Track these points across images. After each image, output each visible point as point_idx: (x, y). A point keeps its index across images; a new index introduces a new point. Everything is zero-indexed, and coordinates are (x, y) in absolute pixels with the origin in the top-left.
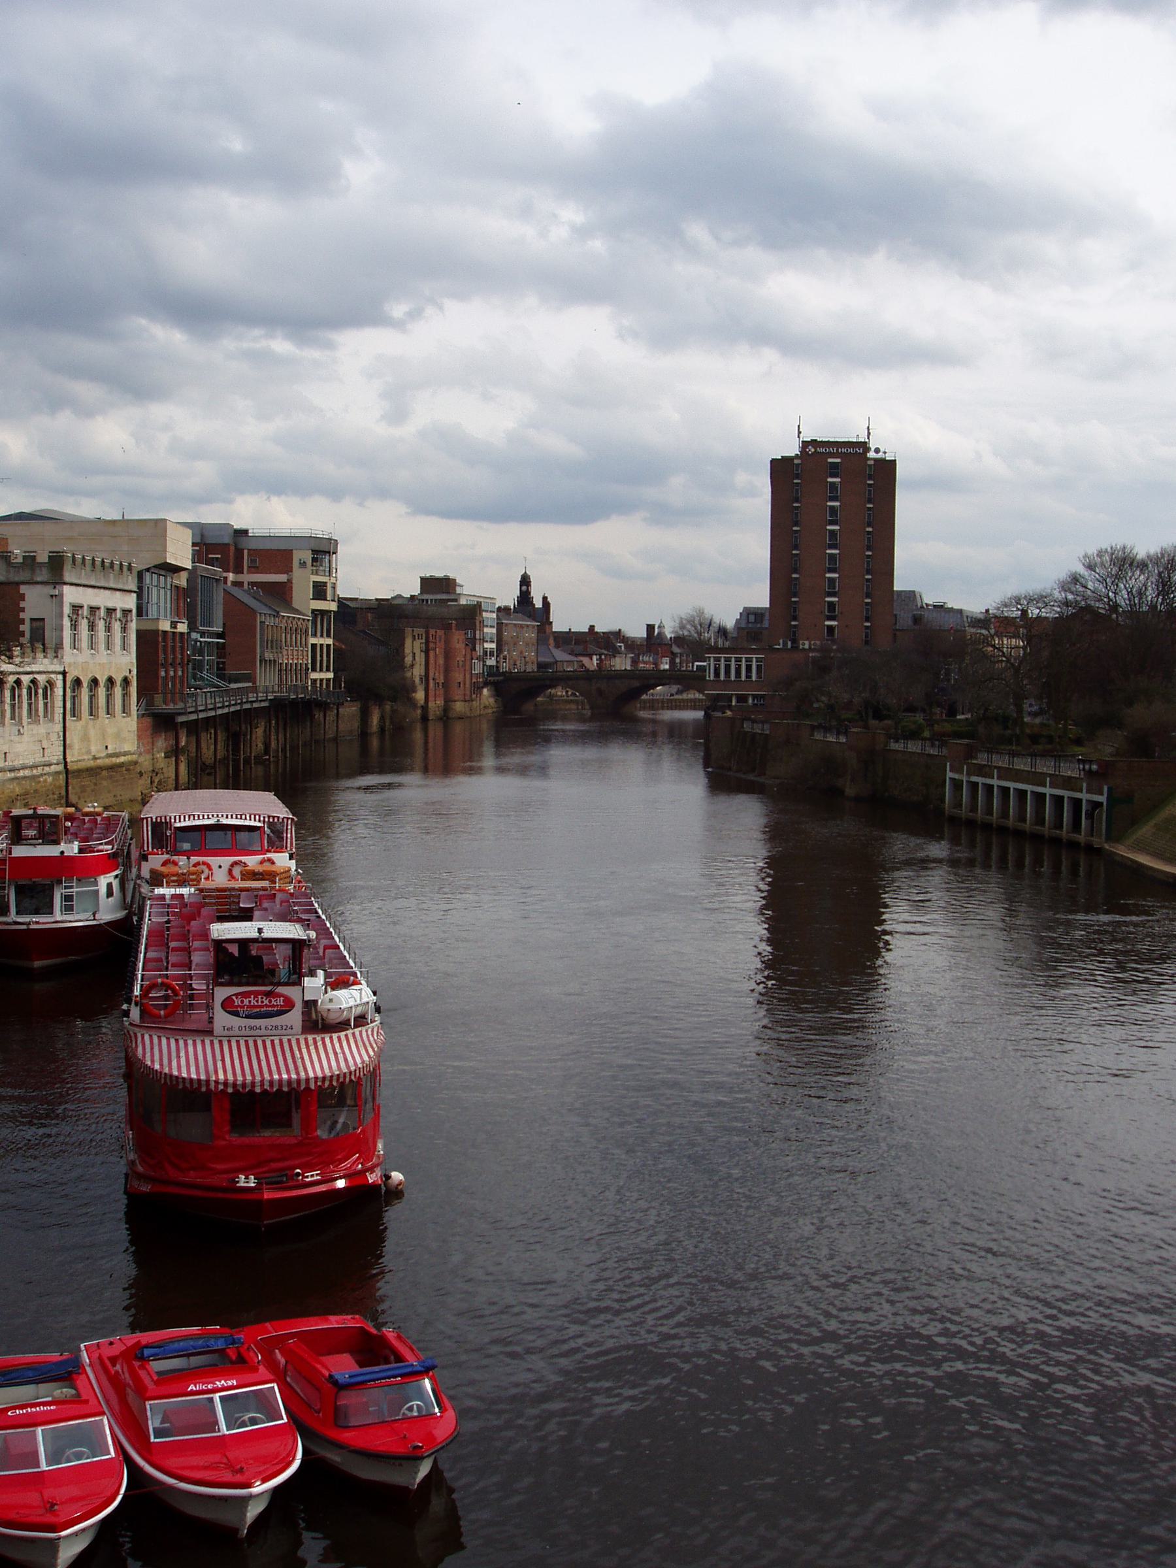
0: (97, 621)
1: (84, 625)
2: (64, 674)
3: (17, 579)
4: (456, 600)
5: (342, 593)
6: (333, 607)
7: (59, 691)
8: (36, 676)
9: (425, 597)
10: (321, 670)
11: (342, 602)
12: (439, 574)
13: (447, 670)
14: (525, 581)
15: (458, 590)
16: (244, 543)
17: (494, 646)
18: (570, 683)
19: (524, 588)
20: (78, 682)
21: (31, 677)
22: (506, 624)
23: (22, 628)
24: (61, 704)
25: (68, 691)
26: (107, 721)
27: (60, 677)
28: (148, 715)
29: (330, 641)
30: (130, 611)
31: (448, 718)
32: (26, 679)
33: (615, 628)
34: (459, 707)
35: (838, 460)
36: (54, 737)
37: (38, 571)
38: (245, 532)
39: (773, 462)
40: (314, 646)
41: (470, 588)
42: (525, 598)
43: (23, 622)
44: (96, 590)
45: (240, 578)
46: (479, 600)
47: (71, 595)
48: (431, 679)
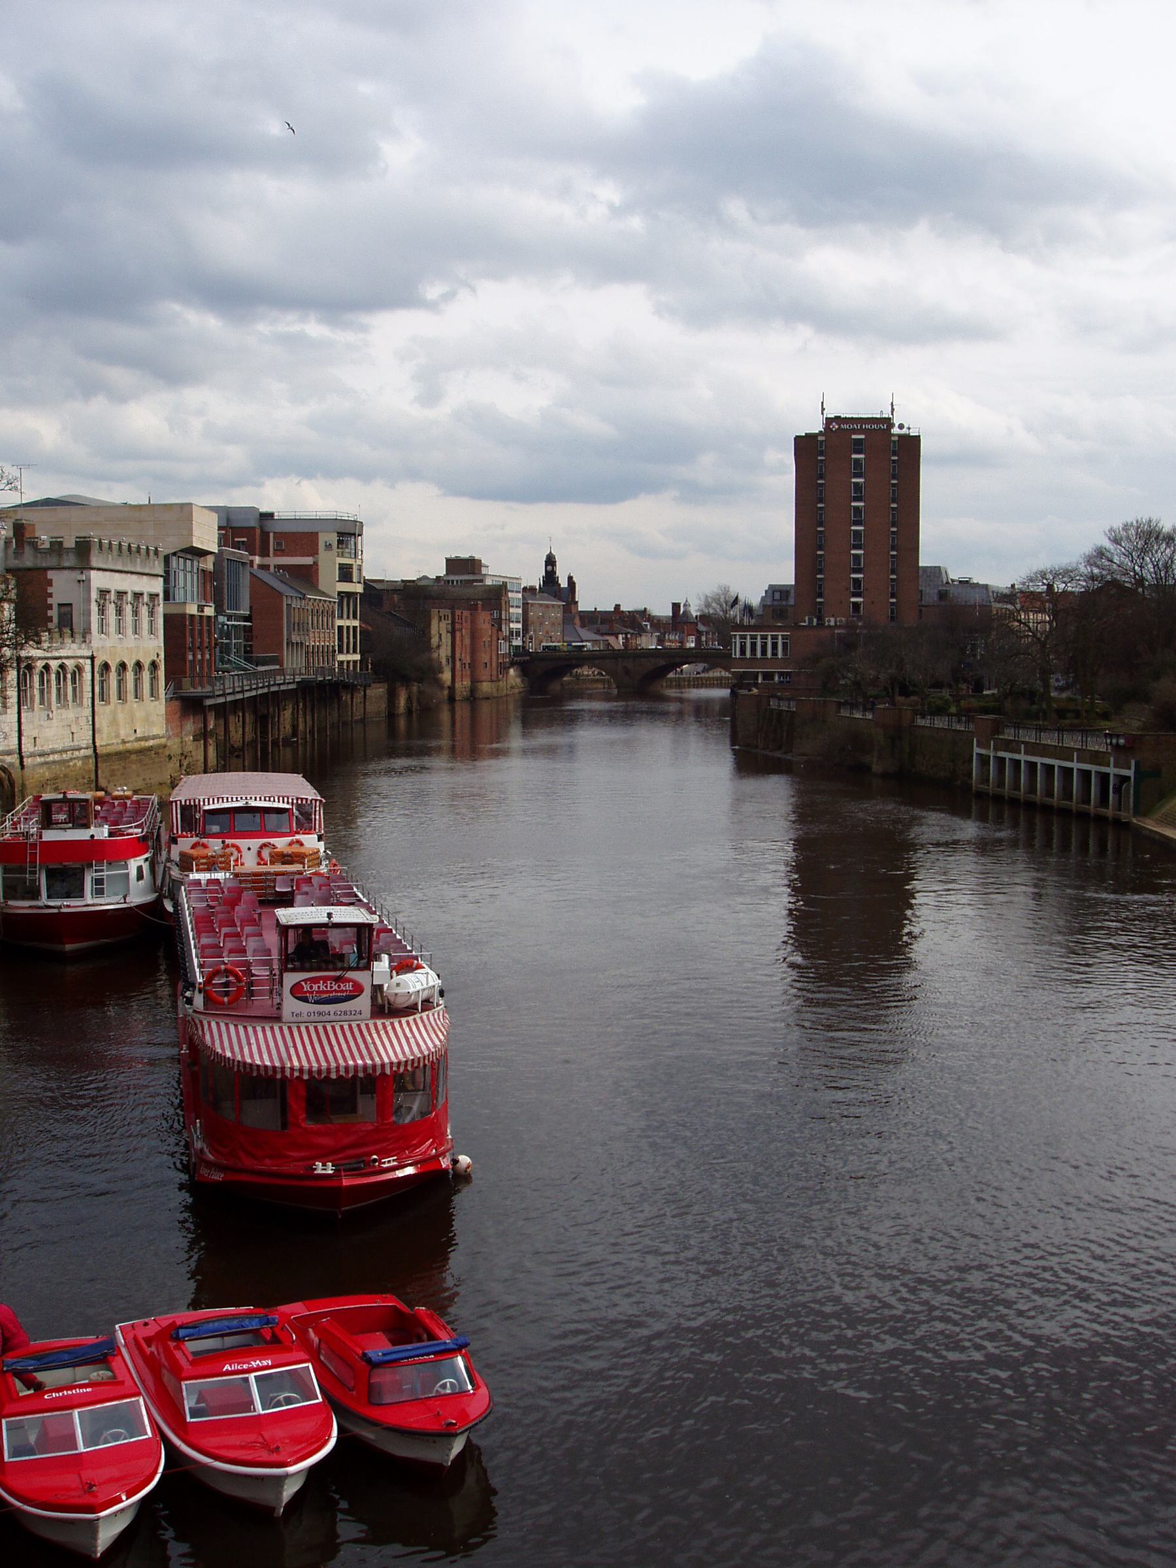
1: (111, 609)
3: (44, 565)
4: (481, 581)
5: (368, 575)
6: (359, 589)
7: (87, 676)
8: (64, 661)
9: (451, 578)
10: (348, 652)
11: (368, 584)
12: (464, 555)
13: (474, 652)
14: (550, 561)
15: (484, 571)
17: (520, 626)
18: (597, 662)
19: (550, 568)
20: (106, 667)
21: (60, 662)
22: (532, 604)
23: (50, 613)
24: (90, 689)
25: (97, 676)
26: (135, 705)
27: (89, 662)
28: (177, 699)
29: (356, 623)
30: (158, 595)
31: (475, 698)
32: (54, 664)
33: (641, 608)
34: (486, 687)
35: (862, 437)
36: (83, 722)
37: (65, 556)
38: (271, 515)
39: (797, 438)
40: (340, 628)
41: (495, 569)
42: (550, 577)
43: (50, 607)
44: (123, 575)
45: (266, 561)
46: (505, 580)
47: (98, 580)
48: (457, 659)
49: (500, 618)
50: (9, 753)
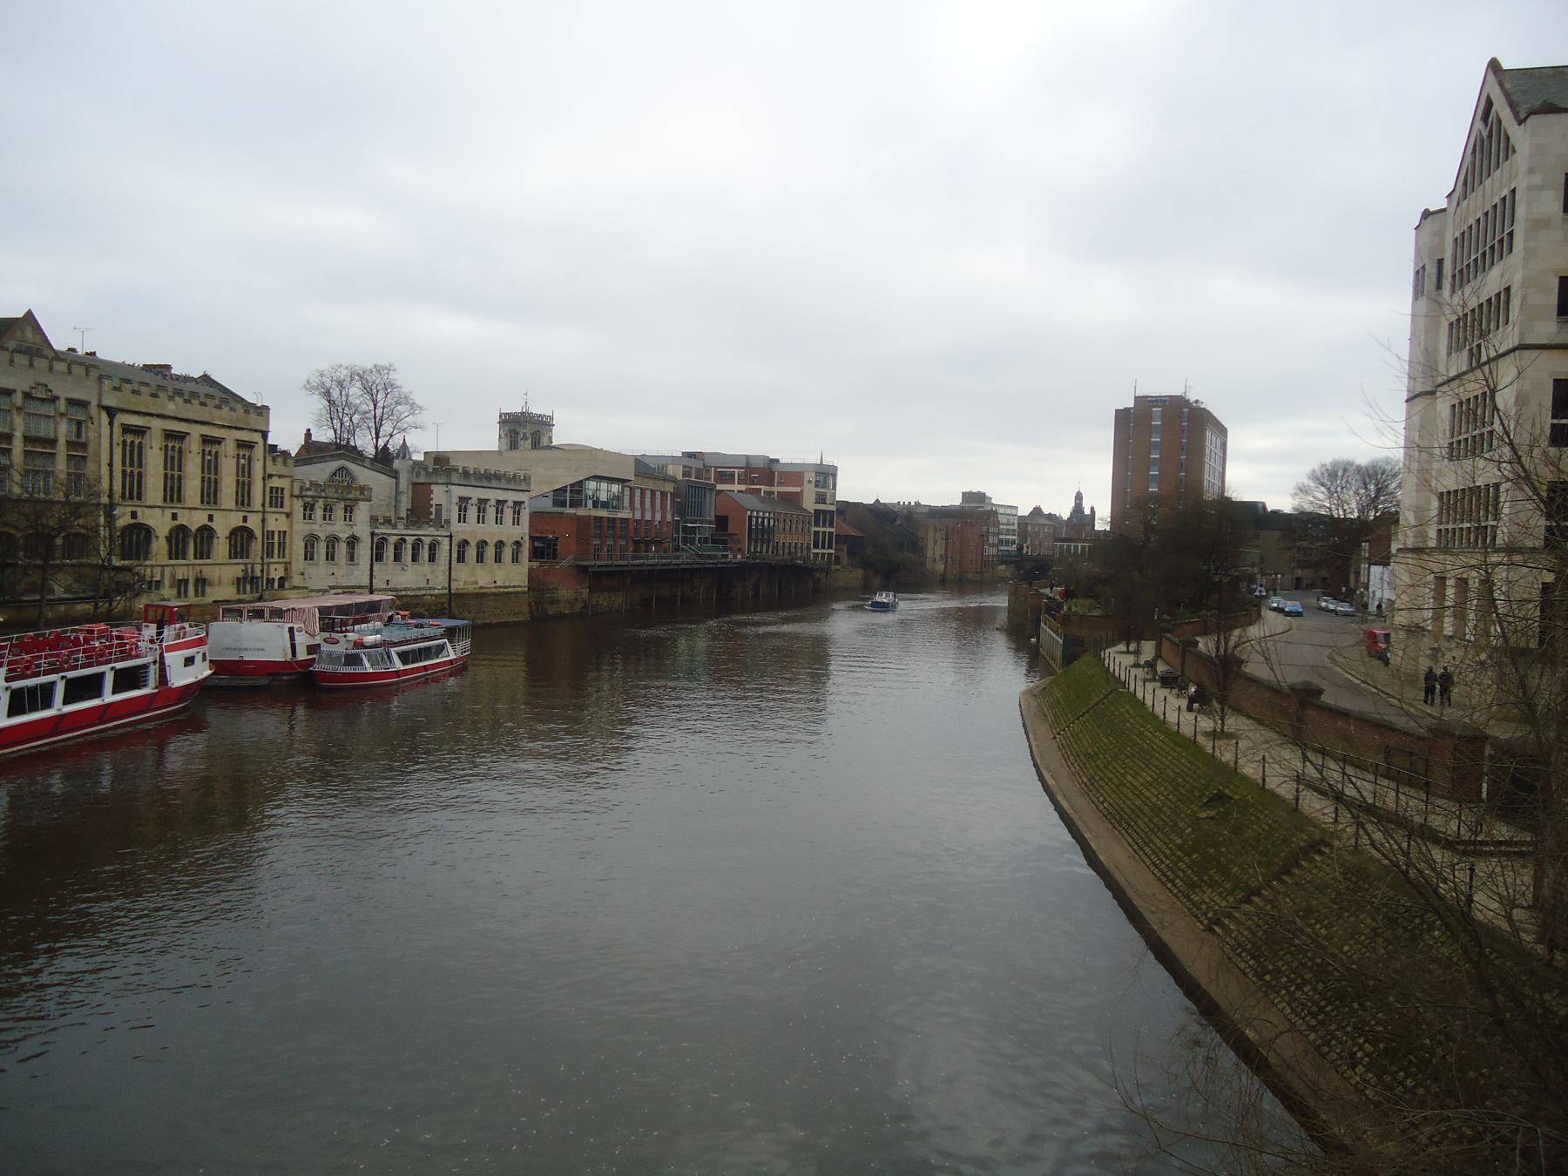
0: (488, 507)
5: (838, 499)
6: (833, 508)
9: (964, 505)
10: (823, 547)
14: (1079, 497)
15: (987, 501)
16: (775, 467)
19: (1078, 502)
21: (430, 539)
27: (448, 539)
29: (833, 530)
32: (410, 540)
36: (441, 573)
38: (778, 461)
40: (816, 533)
42: (1078, 508)
45: (772, 489)
49: (988, 531)
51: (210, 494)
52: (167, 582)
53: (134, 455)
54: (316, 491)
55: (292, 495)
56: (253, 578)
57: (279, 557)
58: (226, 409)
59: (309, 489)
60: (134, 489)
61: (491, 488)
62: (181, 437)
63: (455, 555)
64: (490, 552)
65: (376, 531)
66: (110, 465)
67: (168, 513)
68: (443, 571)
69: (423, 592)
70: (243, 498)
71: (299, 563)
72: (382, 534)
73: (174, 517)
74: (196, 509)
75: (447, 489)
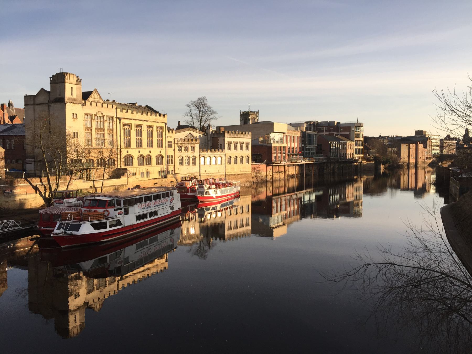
2: (225, 155)
12: (421, 130)
19: (466, 132)
26: (240, 165)
27: (224, 156)
29: (362, 147)
38: (340, 123)
40: (356, 149)
43: (219, 145)
47: (227, 139)
50: (197, 173)
51: (150, 144)
52: (138, 173)
53: (128, 133)
54: (182, 141)
55: (174, 143)
56: (163, 171)
57: (171, 164)
58: (154, 116)
59: (179, 141)
60: (128, 144)
61: (238, 138)
62: (141, 126)
63: (227, 161)
64: (239, 160)
65: (201, 154)
66: (120, 136)
67: (138, 150)
68: (223, 167)
69: (217, 174)
70: (160, 145)
71: (177, 165)
72: (203, 155)
73: (139, 152)
74: (146, 149)
75: (223, 139)
